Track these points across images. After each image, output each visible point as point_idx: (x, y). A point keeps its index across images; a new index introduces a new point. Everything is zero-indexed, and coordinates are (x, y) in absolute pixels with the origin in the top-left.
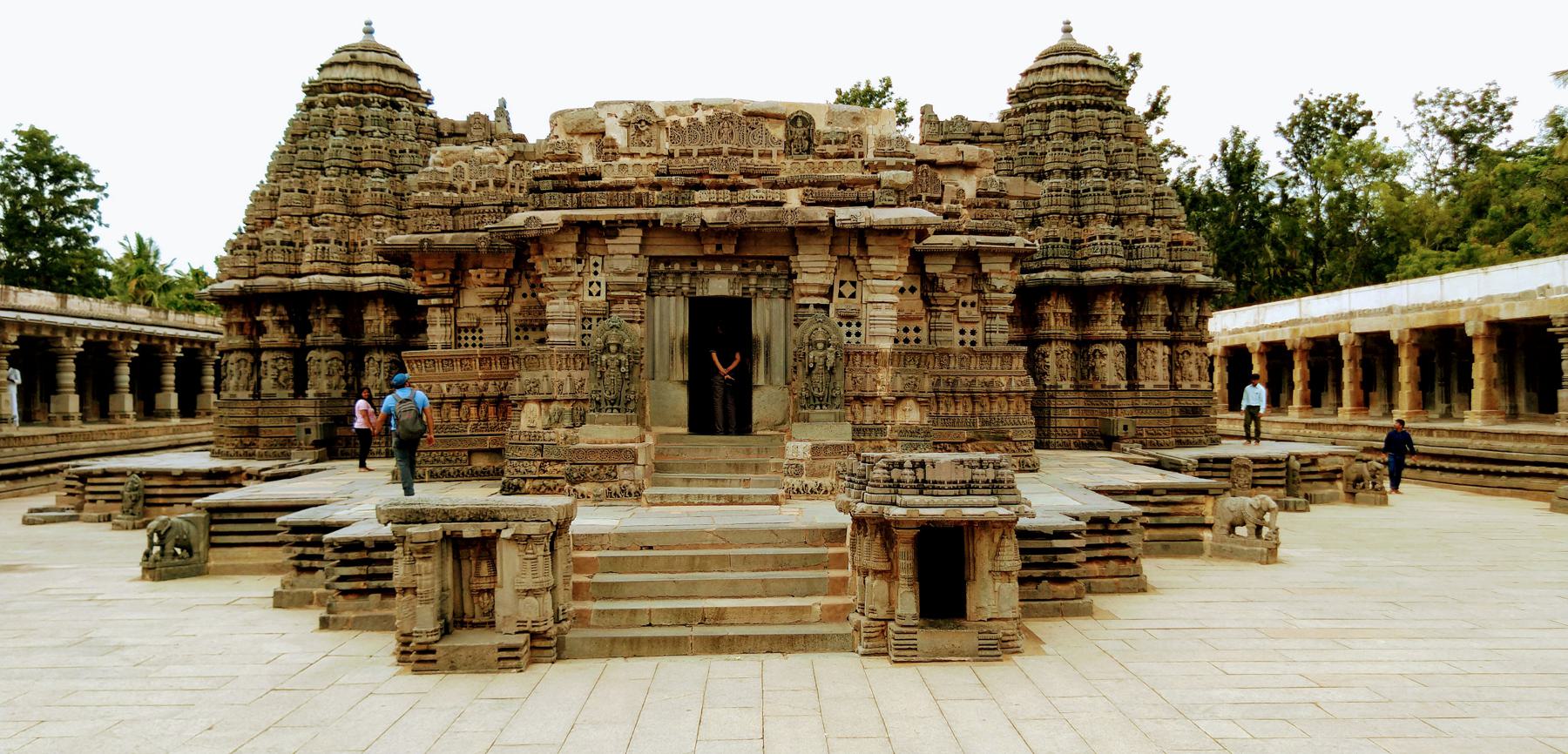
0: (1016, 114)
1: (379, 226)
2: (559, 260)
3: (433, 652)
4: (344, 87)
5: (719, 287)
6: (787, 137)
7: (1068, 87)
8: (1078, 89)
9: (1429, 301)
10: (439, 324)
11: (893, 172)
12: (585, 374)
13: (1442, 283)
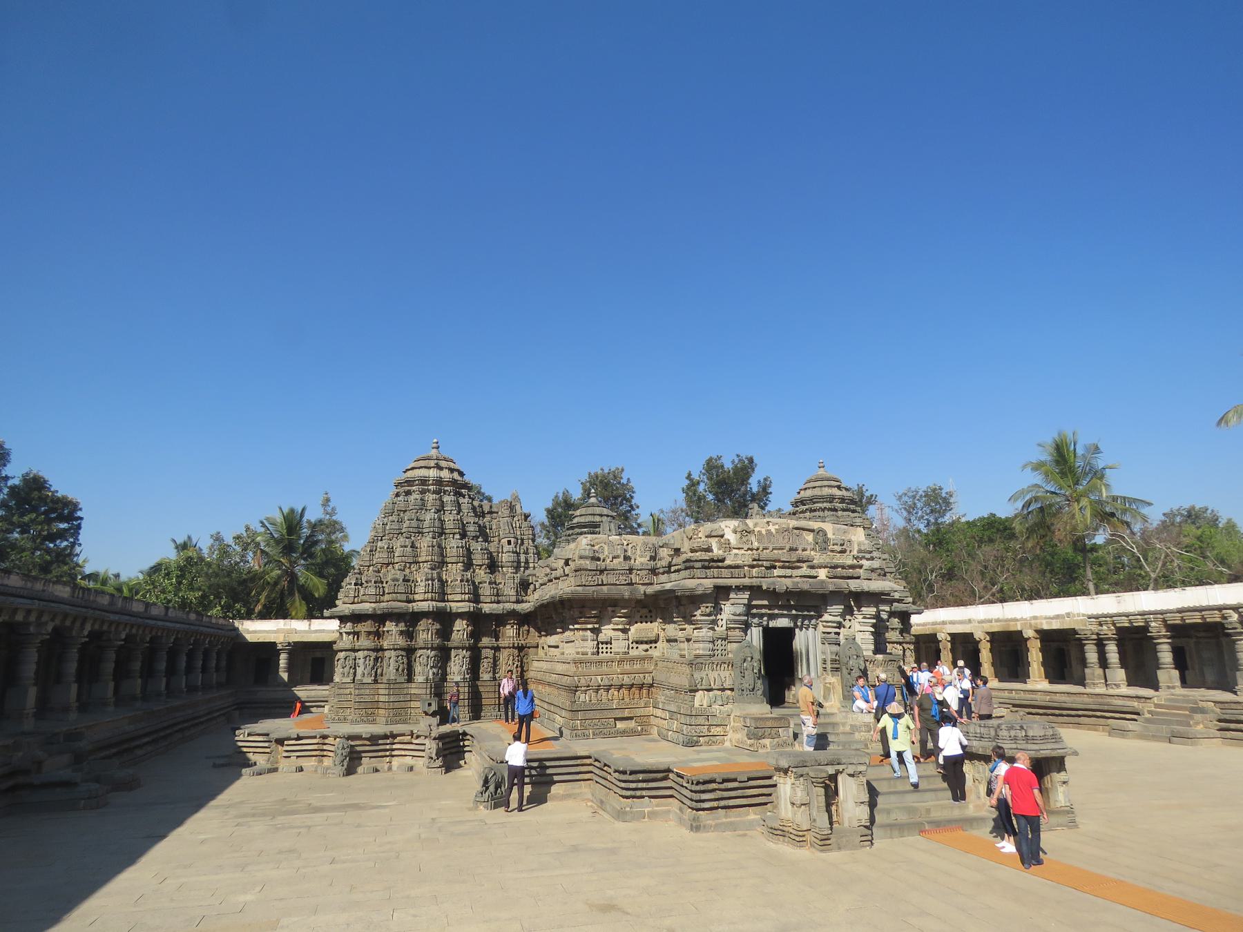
0: (803, 512)
1: (463, 571)
2: (707, 607)
3: (830, 839)
4: (431, 482)
5: (783, 623)
6: (814, 540)
7: (831, 499)
8: (837, 500)
9: (996, 617)
10: (589, 641)
11: (871, 562)
12: (727, 673)
13: (1003, 607)
